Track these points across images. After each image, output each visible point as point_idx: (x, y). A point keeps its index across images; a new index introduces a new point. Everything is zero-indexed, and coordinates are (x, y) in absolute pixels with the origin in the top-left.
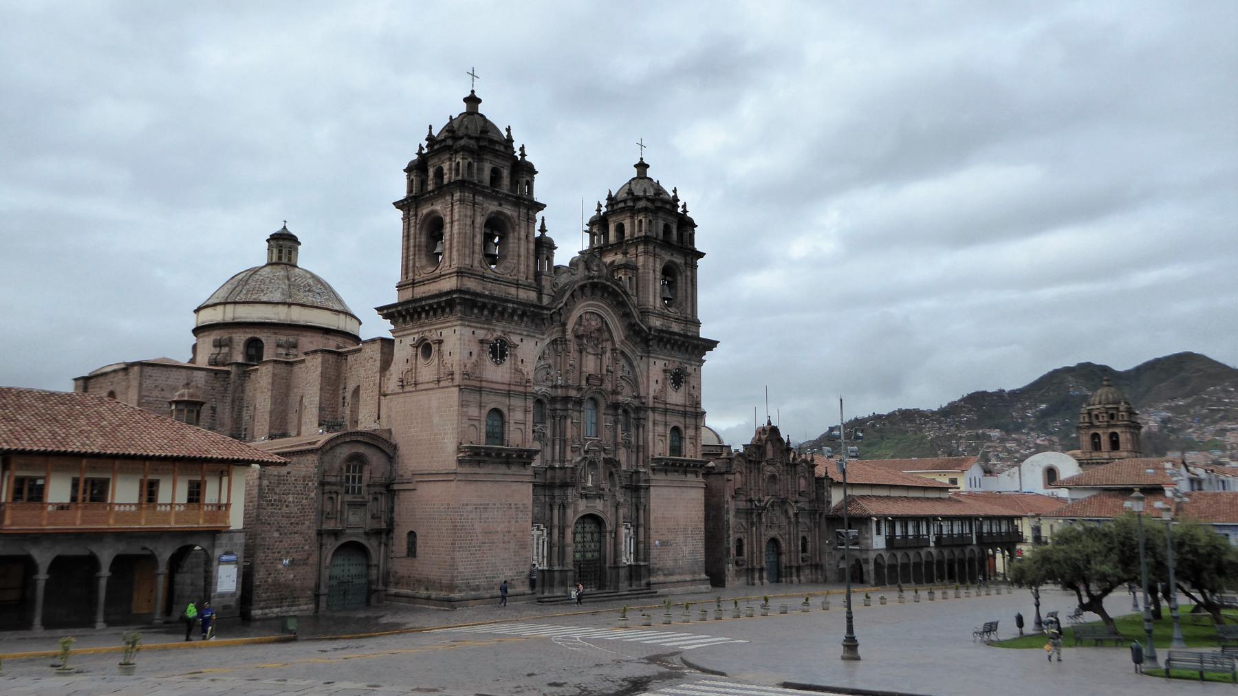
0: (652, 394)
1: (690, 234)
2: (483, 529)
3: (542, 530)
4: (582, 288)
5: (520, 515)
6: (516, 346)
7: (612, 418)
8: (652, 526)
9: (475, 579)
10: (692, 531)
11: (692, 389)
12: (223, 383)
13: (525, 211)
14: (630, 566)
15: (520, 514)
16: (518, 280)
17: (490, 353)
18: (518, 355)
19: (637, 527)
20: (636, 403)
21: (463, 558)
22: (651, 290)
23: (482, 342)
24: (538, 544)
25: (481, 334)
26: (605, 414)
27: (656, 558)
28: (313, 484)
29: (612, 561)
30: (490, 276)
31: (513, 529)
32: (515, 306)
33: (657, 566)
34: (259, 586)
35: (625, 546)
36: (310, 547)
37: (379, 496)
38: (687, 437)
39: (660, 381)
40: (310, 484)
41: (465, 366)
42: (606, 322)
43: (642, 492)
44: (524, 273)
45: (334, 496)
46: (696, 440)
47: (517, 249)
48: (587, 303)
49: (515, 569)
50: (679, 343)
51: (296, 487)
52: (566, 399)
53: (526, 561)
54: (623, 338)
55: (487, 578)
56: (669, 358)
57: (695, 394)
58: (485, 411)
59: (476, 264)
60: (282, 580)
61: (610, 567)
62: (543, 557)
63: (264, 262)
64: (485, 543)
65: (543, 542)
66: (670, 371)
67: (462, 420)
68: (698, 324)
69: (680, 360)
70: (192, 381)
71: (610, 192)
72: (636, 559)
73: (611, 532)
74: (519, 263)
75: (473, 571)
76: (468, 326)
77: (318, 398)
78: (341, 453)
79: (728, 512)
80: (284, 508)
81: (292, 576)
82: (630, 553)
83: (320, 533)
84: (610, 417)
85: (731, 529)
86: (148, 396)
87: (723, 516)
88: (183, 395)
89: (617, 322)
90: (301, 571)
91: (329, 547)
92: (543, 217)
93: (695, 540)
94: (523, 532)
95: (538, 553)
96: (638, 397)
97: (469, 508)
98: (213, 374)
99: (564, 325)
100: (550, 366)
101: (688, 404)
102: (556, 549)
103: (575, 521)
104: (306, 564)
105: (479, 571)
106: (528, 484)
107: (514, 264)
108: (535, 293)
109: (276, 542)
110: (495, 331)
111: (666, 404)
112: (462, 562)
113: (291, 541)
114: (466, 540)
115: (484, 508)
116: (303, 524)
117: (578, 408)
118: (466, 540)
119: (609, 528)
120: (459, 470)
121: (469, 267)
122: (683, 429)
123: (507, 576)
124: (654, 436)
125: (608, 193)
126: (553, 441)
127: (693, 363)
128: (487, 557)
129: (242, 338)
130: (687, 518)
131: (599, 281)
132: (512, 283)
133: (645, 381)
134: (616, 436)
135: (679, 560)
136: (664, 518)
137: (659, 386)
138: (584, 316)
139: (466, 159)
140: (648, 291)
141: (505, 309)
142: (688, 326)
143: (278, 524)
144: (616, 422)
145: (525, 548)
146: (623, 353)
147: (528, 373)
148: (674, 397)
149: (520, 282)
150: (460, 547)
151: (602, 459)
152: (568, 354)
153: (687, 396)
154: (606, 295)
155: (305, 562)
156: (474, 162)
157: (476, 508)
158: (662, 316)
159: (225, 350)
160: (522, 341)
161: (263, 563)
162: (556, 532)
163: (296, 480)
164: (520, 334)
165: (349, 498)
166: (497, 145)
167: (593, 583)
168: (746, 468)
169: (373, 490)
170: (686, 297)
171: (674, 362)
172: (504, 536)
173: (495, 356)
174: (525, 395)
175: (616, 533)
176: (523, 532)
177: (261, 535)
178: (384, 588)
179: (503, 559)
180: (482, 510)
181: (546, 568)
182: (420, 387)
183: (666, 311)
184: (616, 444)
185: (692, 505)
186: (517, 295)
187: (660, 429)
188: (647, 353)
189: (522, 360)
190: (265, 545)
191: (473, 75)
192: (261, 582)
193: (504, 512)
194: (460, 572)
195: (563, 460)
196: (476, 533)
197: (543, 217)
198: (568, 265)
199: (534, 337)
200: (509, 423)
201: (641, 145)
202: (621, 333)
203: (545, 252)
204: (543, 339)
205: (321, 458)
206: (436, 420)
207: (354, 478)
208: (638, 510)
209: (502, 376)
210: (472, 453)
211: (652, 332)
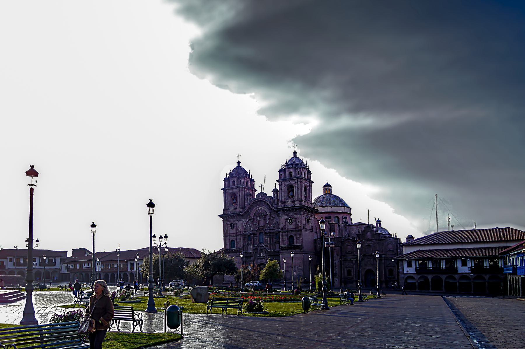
6: (236, 224)
42: (265, 210)
57: (299, 224)
63: (323, 194)
100: (251, 226)
137: (284, 224)
148: (290, 227)
173: (231, 227)
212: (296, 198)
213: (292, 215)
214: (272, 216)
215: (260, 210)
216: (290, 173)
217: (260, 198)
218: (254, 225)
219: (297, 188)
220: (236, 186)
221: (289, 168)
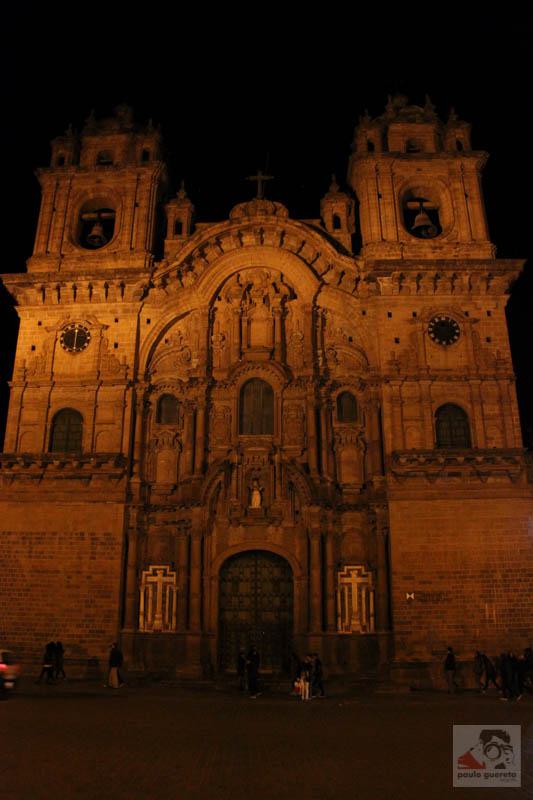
3: (172, 576)
5: (99, 548)
8: (396, 566)
9: (16, 634)
10: (504, 576)
11: (483, 342)
13: (135, 177)
15: (99, 547)
17: (61, 342)
24: (164, 595)
27: (410, 623)
31: (85, 569)
35: (360, 604)
39: (403, 338)
55: (36, 635)
57: (493, 348)
64: (37, 585)
73: (299, 579)
75: (13, 624)
94: (104, 573)
95: (163, 609)
97: (13, 538)
103: (220, 562)
115: (37, 538)
119: (297, 572)
122: (469, 406)
123: (73, 636)
128: (37, 605)
135: (474, 626)
145: (109, 597)
147: (125, 358)
153: (472, 353)
157: (23, 538)
160: (116, 321)
162: (183, 575)
164: (113, 312)
172: (69, 577)
176: (104, 573)
180: (34, 541)
189: (116, 345)
193: (71, 543)
209: (81, 368)
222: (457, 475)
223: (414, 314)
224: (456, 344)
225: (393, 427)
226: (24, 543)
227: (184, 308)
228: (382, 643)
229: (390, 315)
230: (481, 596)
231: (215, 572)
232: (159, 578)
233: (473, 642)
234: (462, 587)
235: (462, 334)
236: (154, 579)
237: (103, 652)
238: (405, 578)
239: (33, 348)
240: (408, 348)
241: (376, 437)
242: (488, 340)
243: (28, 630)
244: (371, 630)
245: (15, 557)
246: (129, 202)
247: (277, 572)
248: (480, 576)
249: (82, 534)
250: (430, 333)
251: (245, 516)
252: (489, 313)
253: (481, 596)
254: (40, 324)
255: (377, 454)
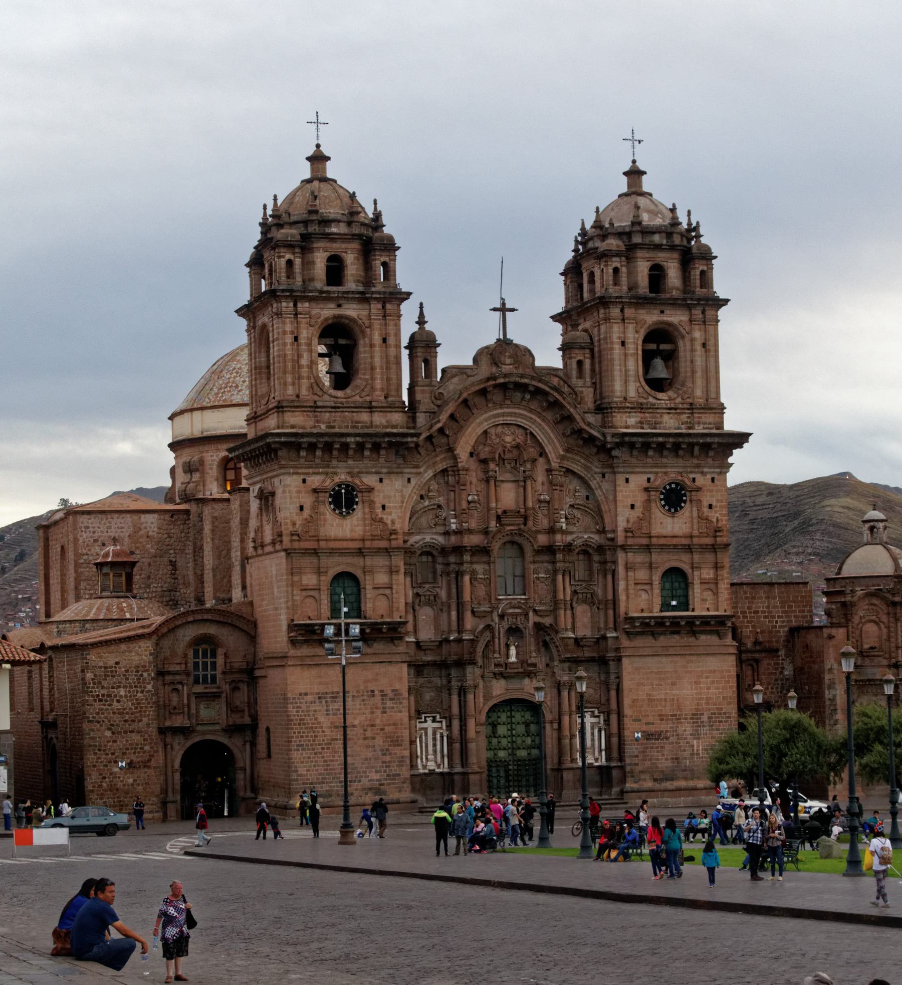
0: (622, 524)
1: (703, 273)
2: (331, 723)
4: (483, 392)
5: (389, 704)
6: (371, 490)
7: (550, 567)
8: (627, 711)
9: (323, 783)
10: (710, 718)
12: (181, 527)
13: (380, 306)
14: (599, 767)
16: (371, 402)
18: (376, 499)
19: (608, 714)
20: (596, 538)
21: (304, 758)
22: (617, 373)
23: (315, 491)
24: (434, 739)
25: (315, 481)
26: (534, 562)
27: (637, 756)
28: (149, 675)
29: (556, 760)
30: (328, 404)
31: (378, 721)
32: (358, 439)
33: (640, 768)
34: (92, 791)
35: (593, 740)
36: (152, 748)
37: (241, 685)
38: (697, 581)
39: (637, 505)
40: (145, 675)
41: (294, 524)
42: (531, 433)
43: (612, 665)
44: (382, 390)
45: (179, 687)
46: (717, 584)
47: (369, 360)
48: (496, 412)
49: (385, 771)
50: (669, 446)
51: (127, 679)
52: (458, 550)
53: (400, 762)
54: (562, 453)
56: (655, 470)
57: (714, 515)
58: (327, 579)
59: (304, 392)
60: (120, 785)
61: (552, 769)
62: (443, 757)
65: (442, 737)
66: (656, 489)
67: (293, 591)
68: (720, 409)
69: (681, 470)
70: (140, 529)
71: (583, 224)
72: (608, 759)
73: (551, 722)
74: (373, 379)
75: (320, 774)
76: (294, 473)
77: (239, 553)
78: (184, 636)
79: (831, 686)
80: (115, 703)
81: (131, 781)
82: (600, 751)
83: (162, 731)
84: (545, 565)
85: (839, 711)
86: (87, 554)
87: (824, 693)
88: (107, 555)
89: (549, 431)
90: (142, 775)
91: (176, 747)
92: (421, 304)
93: (718, 730)
94: (395, 724)
95: (435, 751)
96: (602, 531)
97: (309, 698)
98: (167, 517)
99: (451, 450)
100: (439, 507)
101: (696, 533)
102: (457, 746)
103: (486, 709)
104: (149, 767)
105: (327, 774)
106: (400, 665)
107: (366, 380)
108: (401, 414)
109: (109, 742)
110: (336, 473)
111: (650, 537)
112: (302, 762)
113: (127, 741)
114: (307, 736)
116: (140, 721)
117: (485, 559)
118: (307, 736)
119: (548, 716)
120: (292, 652)
121: (294, 398)
122: (690, 571)
124: (627, 585)
125: (580, 226)
126: (449, 607)
127: (706, 470)
129: (215, 457)
130: (700, 699)
131: (507, 380)
132: (361, 407)
133: (612, 507)
134: (555, 591)
135: (685, 758)
136: (651, 700)
137: (638, 512)
138: (492, 431)
139: (284, 257)
140: (612, 376)
141: (345, 447)
142: (696, 415)
143: (109, 721)
144: (555, 572)
146: (569, 471)
147: (393, 522)
149: (374, 404)
150: (298, 745)
151: (531, 624)
152: (462, 488)
153: (695, 521)
154: (528, 396)
155: (146, 764)
156: (295, 257)
157: (319, 698)
158: (640, 408)
159: (196, 476)
160: (381, 480)
161: (94, 766)
162: (456, 723)
163: (127, 671)
164: (376, 473)
165: (199, 689)
166: (333, 225)
167: (532, 789)
168: (888, 614)
169: (230, 678)
170: (693, 372)
171: (666, 473)
172: (365, 730)
174: (387, 551)
175: (559, 724)
176: (395, 724)
177: (89, 734)
178: (253, 795)
179: (366, 759)
181: (446, 770)
182: (269, 549)
183: (651, 400)
184: (555, 602)
185: (709, 680)
186: (371, 422)
187: (642, 575)
188: (610, 467)
189: (384, 507)
190: (95, 746)
191: (317, 123)
192: (94, 786)
194: (301, 775)
195: (460, 630)
196: (321, 727)
197: (421, 304)
198: (470, 363)
199: (402, 473)
200: (365, 588)
201: (633, 140)
202: (558, 445)
203: (419, 354)
204: (420, 473)
205: (157, 644)
206: (276, 590)
207: (205, 664)
208: (608, 691)
209: (352, 531)
210: (303, 632)
211: (609, 439)
212: (698, 392)
213: (681, 473)
214: (566, 464)
215: (506, 430)
216: (657, 275)
217: (506, 369)
218: (469, 502)
219: (698, 347)
220: (351, 285)
221: (658, 247)
222: (678, 633)
223: (649, 480)
224: (682, 511)
225: (627, 589)
226: (321, 702)
227: (440, 465)
228: (615, 773)
229: (627, 480)
230: (691, 734)
231: (483, 718)
232: (430, 725)
233: (685, 770)
234: (677, 727)
235: (688, 502)
236: (424, 725)
237: (400, 791)
238: (634, 720)
239: (301, 508)
240: (641, 516)
241: (610, 597)
242: (710, 506)
243: (334, 778)
244: (603, 761)
245: (314, 715)
246: (377, 338)
247: (528, 716)
248: (691, 718)
249: (373, 691)
250: (661, 500)
251: (504, 673)
252: (713, 480)
253: (691, 734)
254: (304, 481)
255: (611, 612)
